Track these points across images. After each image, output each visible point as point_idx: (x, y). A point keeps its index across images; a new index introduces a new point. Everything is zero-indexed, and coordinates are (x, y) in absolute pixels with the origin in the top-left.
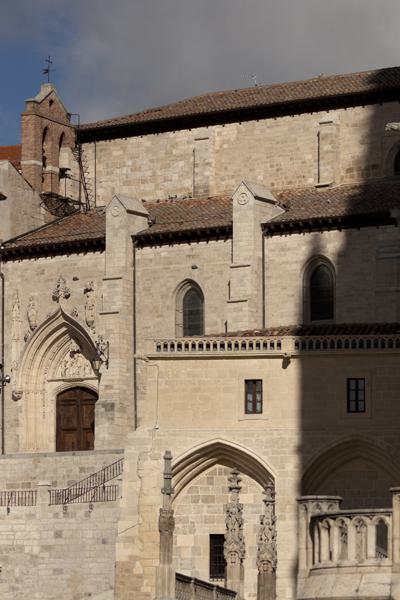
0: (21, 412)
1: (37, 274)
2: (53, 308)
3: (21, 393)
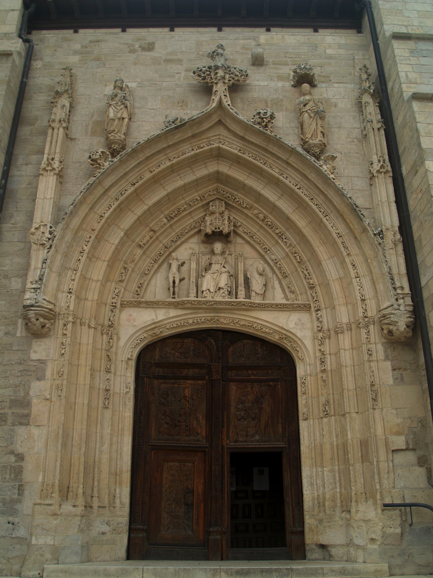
1: (133, 51)
2: (194, 109)
3: (51, 316)
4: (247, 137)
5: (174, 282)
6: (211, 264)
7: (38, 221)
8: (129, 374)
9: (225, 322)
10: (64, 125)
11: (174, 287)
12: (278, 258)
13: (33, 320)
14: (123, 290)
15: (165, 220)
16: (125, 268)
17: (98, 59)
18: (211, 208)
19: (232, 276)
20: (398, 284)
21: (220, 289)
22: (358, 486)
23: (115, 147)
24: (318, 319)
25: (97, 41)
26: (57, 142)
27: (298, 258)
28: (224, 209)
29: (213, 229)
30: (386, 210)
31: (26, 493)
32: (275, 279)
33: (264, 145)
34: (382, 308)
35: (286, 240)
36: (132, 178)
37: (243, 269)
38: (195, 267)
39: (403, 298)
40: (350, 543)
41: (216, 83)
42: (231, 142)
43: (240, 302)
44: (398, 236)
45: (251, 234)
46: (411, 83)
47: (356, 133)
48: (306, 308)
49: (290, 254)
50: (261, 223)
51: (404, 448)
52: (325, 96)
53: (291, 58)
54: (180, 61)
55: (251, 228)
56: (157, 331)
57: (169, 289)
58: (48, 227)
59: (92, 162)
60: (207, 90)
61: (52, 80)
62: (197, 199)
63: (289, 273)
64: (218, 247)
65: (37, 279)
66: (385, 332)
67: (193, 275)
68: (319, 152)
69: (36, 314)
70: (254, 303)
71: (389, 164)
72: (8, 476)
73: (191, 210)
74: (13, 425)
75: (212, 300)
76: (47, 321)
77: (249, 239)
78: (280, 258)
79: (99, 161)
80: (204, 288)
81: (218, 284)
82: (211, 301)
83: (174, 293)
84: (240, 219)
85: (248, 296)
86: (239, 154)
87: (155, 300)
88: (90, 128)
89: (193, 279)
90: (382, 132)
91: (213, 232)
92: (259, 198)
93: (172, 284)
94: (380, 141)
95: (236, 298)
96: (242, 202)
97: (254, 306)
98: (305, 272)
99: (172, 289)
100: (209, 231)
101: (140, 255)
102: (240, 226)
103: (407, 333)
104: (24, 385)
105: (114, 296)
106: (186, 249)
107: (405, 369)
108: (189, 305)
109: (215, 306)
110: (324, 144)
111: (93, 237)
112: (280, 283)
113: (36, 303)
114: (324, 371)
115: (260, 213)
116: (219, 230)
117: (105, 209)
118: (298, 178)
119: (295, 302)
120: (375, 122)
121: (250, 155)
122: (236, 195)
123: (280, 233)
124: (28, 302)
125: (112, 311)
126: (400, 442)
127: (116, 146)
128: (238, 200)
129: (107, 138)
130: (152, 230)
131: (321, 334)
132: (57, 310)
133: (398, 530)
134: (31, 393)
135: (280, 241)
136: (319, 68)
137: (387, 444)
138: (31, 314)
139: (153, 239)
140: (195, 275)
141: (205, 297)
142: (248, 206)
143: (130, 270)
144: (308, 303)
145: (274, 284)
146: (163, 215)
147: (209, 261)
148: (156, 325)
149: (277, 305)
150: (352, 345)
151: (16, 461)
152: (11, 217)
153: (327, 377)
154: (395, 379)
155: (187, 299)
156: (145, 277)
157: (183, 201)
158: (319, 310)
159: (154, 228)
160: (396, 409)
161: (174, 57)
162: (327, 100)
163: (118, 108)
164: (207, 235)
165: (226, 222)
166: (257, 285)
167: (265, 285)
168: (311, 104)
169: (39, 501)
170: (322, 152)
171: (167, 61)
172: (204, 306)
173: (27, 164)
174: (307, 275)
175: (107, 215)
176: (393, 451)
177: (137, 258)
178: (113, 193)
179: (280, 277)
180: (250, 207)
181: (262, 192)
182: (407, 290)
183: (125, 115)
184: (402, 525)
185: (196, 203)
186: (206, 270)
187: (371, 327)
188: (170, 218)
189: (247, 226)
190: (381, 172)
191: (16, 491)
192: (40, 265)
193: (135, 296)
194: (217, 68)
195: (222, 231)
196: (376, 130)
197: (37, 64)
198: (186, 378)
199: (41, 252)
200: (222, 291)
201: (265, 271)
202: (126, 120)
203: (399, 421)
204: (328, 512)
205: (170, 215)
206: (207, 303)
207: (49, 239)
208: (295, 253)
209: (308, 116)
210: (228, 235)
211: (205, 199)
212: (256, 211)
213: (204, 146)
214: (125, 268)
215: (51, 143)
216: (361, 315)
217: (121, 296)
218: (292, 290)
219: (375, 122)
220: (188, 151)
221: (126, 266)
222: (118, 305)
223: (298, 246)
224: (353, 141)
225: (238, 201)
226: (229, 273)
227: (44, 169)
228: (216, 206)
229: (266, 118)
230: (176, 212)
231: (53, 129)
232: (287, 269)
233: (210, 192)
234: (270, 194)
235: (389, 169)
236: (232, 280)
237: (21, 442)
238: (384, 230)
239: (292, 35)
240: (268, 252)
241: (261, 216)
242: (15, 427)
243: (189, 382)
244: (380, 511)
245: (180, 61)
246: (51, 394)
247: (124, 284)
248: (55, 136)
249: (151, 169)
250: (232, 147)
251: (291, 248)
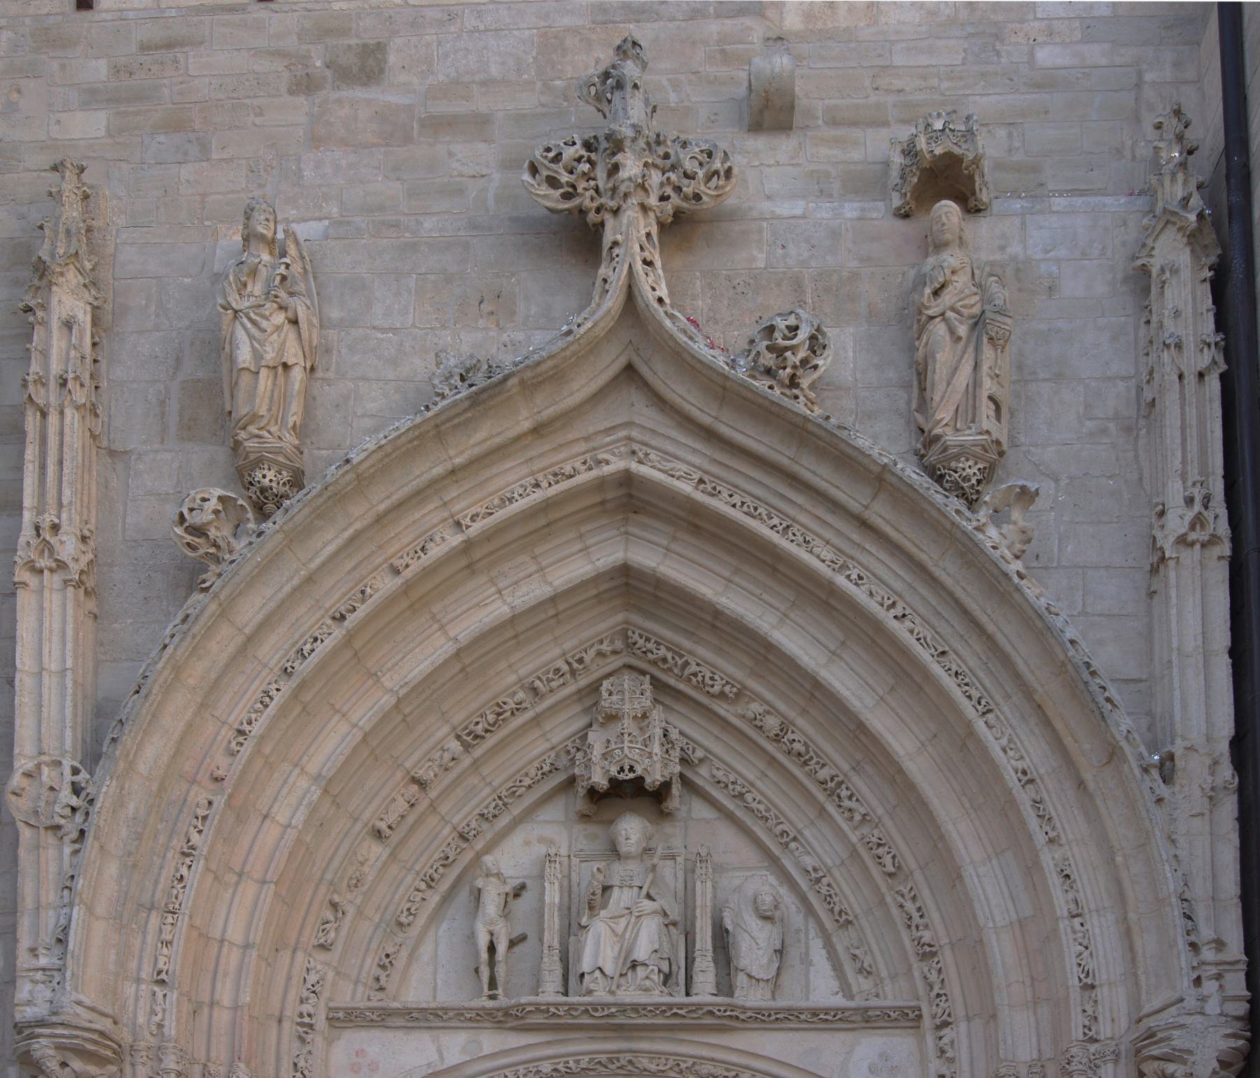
5: (492, 949)
12: (825, 865)
15: (455, 746)
19: (674, 924)
21: (634, 965)
28: (648, 703)
29: (614, 771)
32: (812, 933)
35: (853, 804)
37: (709, 904)
38: (557, 900)
43: (699, 1006)
45: (738, 788)
50: (770, 747)
55: (740, 768)
57: (477, 970)
62: (557, 670)
63: (858, 910)
67: (553, 923)
70: (745, 1009)
73: (539, 709)
78: (829, 862)
80: (586, 966)
81: (629, 952)
82: (609, 1005)
83: (493, 984)
85: (725, 986)
87: (433, 1005)
89: (552, 937)
91: (612, 781)
93: (484, 956)
95: (688, 994)
96: (708, 675)
97: (742, 1017)
101: (379, 864)
102: (701, 761)
109: (621, 1020)
115: (768, 713)
116: (631, 776)
119: (874, 1002)
122: (690, 653)
123: (832, 780)
128: (693, 668)
130: (415, 780)
135: (831, 808)
140: (557, 926)
141: (590, 992)
142: (727, 689)
145: (807, 948)
146: (446, 729)
147: (601, 877)
149: (815, 1013)
155: (532, 999)
156: (401, 935)
157: (512, 678)
159: (420, 773)
165: (657, 749)
166: (754, 949)
167: (780, 952)
180: (736, 694)
185: (554, 684)
188: (469, 739)
193: (372, 993)
200: (641, 972)
201: (782, 906)
205: (472, 727)
206: (597, 1010)
208: (879, 845)
212: (756, 707)
218: (865, 965)
225: (695, 675)
226: (665, 914)
228: (621, 692)
230: (491, 718)
232: (852, 897)
233: (601, 642)
236: (674, 937)
240: (793, 845)
251: (865, 830)
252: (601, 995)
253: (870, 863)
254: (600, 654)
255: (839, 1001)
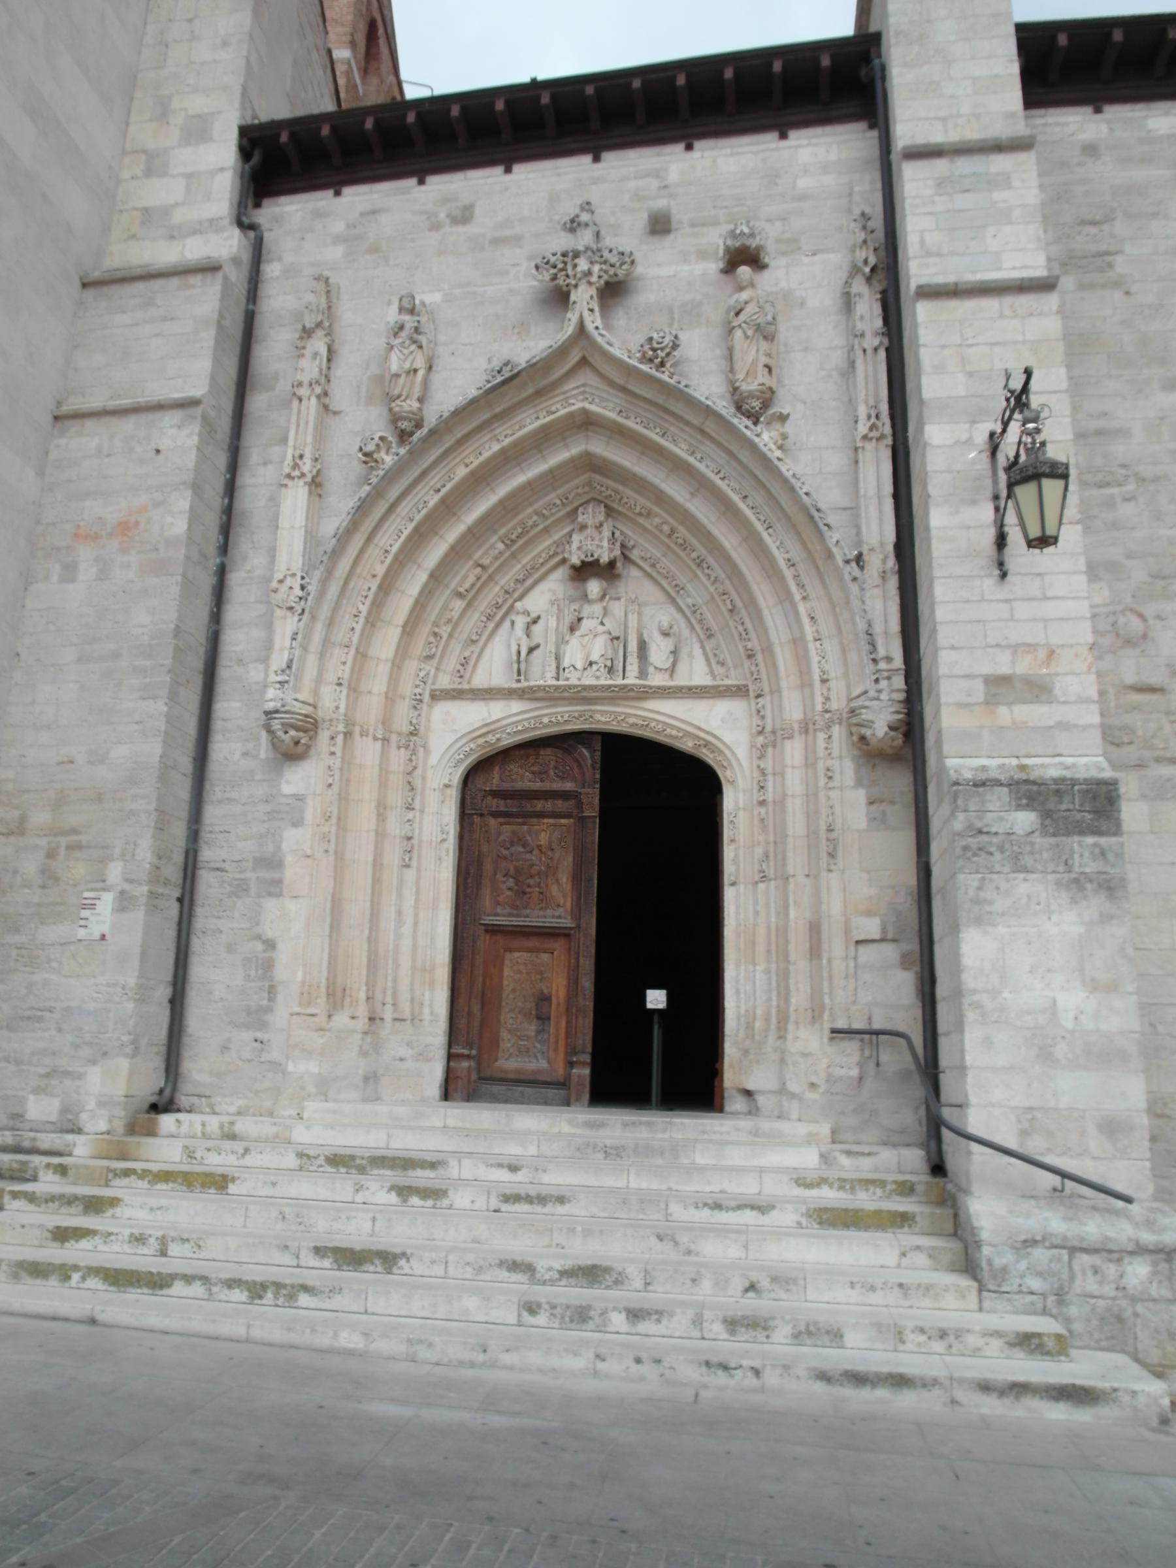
0: (297, 823)
1: (436, 227)
3: (310, 726)
4: (631, 387)
5: (519, 653)
6: (580, 620)
7: (283, 568)
8: (446, 811)
9: (603, 719)
10: (318, 390)
11: (519, 662)
13: (280, 733)
14: (433, 671)
15: (501, 546)
16: (435, 634)
17: (374, 249)
18: (580, 519)
20: (882, 652)
21: (591, 664)
22: (799, 999)
23: (404, 425)
24: (759, 712)
25: (374, 212)
26: (307, 423)
27: (728, 602)
29: (583, 557)
30: (873, 513)
31: (280, 997)
33: (660, 400)
34: (854, 694)
36: (434, 479)
39: (888, 678)
40: (782, 1090)
41: (576, 286)
42: (605, 396)
44: (891, 562)
46: (929, 254)
47: (837, 358)
48: (740, 691)
49: (716, 597)
51: (877, 936)
52: (783, 285)
53: (726, 207)
54: (517, 240)
56: (491, 738)
58: (299, 578)
59: (364, 458)
60: (560, 298)
61: (300, 299)
63: (716, 628)
64: (594, 587)
65: (284, 665)
66: (855, 738)
68: (757, 407)
69: (283, 724)
71: (888, 421)
72: (253, 973)
74: (259, 897)
75: (578, 683)
76: (301, 734)
77: (648, 569)
79: (375, 456)
82: (576, 686)
83: (519, 674)
84: (633, 536)
86: (620, 420)
88: (364, 389)
89: (551, 647)
90: (882, 354)
91: (583, 562)
92: (660, 498)
93: (515, 658)
94: (876, 372)
98: (740, 628)
99: (515, 666)
100: (575, 560)
103: (893, 739)
104: (273, 835)
105: (418, 683)
106: (542, 592)
107: (892, 803)
108: (541, 694)
109: (584, 694)
110: (770, 389)
111: (374, 588)
112: (703, 647)
113: (283, 706)
114: (763, 803)
116: (591, 559)
117: (392, 537)
118: (722, 457)
120: (868, 334)
121: (638, 420)
124: (271, 706)
125: (415, 708)
126: (871, 927)
127: (405, 423)
128: (625, 500)
129: (390, 410)
131: (761, 739)
132: (320, 714)
133: (855, 1072)
134: (285, 847)
135: (699, 573)
136: (779, 224)
137: (847, 930)
138: (276, 725)
139: (483, 579)
141: (567, 679)
143: (445, 636)
144: (744, 682)
148: (489, 728)
149: (690, 688)
150: (806, 759)
151: (264, 951)
152: (245, 559)
153: (767, 813)
154: (872, 820)
158: (759, 696)
160: (868, 872)
161: (507, 232)
162: (787, 295)
163: (406, 351)
164: (573, 567)
165: (605, 543)
166: (659, 653)
168: (750, 309)
169: (297, 1010)
170: (766, 405)
171: (497, 242)
172: (566, 694)
173: (265, 464)
174: (744, 633)
175: (395, 549)
176: (858, 942)
177: (455, 615)
178: (404, 509)
179: (702, 636)
181: (664, 486)
182: (898, 662)
183: (420, 363)
184: (861, 1065)
186: (572, 629)
187: (836, 730)
188: (509, 542)
189: (644, 548)
190: (871, 439)
191: (266, 995)
192: (287, 643)
194: (577, 255)
195: (598, 560)
196: (869, 352)
197: (271, 270)
198: (541, 815)
199: (289, 621)
200: (595, 667)
202: (421, 373)
203: (872, 891)
204: (757, 1038)
207: (300, 599)
209: (743, 336)
210: (612, 564)
211: (571, 502)
213: (558, 410)
214: (435, 634)
215: (298, 425)
216: (819, 707)
217: (430, 681)
219: (868, 334)
220: (530, 422)
221: (436, 630)
222: (426, 697)
223: (727, 582)
224: (830, 376)
226: (610, 633)
227: (289, 476)
229: (662, 349)
231: (300, 400)
234: (676, 490)
235: (888, 430)
237: (272, 922)
238: (865, 552)
239: (732, 155)
241: (666, 528)
242: (262, 900)
243: (546, 820)
244: (826, 1040)
245: (517, 240)
246: (311, 848)
247: (435, 662)
248: (304, 412)
249: (467, 461)
250: (606, 408)
251: (717, 585)
252: (574, 681)
253: (720, 603)
254: (577, 494)
255: (707, 681)
